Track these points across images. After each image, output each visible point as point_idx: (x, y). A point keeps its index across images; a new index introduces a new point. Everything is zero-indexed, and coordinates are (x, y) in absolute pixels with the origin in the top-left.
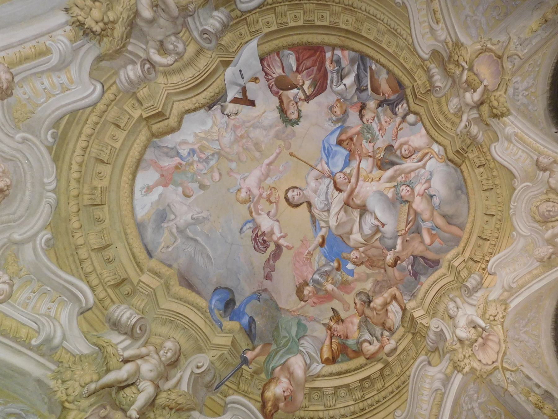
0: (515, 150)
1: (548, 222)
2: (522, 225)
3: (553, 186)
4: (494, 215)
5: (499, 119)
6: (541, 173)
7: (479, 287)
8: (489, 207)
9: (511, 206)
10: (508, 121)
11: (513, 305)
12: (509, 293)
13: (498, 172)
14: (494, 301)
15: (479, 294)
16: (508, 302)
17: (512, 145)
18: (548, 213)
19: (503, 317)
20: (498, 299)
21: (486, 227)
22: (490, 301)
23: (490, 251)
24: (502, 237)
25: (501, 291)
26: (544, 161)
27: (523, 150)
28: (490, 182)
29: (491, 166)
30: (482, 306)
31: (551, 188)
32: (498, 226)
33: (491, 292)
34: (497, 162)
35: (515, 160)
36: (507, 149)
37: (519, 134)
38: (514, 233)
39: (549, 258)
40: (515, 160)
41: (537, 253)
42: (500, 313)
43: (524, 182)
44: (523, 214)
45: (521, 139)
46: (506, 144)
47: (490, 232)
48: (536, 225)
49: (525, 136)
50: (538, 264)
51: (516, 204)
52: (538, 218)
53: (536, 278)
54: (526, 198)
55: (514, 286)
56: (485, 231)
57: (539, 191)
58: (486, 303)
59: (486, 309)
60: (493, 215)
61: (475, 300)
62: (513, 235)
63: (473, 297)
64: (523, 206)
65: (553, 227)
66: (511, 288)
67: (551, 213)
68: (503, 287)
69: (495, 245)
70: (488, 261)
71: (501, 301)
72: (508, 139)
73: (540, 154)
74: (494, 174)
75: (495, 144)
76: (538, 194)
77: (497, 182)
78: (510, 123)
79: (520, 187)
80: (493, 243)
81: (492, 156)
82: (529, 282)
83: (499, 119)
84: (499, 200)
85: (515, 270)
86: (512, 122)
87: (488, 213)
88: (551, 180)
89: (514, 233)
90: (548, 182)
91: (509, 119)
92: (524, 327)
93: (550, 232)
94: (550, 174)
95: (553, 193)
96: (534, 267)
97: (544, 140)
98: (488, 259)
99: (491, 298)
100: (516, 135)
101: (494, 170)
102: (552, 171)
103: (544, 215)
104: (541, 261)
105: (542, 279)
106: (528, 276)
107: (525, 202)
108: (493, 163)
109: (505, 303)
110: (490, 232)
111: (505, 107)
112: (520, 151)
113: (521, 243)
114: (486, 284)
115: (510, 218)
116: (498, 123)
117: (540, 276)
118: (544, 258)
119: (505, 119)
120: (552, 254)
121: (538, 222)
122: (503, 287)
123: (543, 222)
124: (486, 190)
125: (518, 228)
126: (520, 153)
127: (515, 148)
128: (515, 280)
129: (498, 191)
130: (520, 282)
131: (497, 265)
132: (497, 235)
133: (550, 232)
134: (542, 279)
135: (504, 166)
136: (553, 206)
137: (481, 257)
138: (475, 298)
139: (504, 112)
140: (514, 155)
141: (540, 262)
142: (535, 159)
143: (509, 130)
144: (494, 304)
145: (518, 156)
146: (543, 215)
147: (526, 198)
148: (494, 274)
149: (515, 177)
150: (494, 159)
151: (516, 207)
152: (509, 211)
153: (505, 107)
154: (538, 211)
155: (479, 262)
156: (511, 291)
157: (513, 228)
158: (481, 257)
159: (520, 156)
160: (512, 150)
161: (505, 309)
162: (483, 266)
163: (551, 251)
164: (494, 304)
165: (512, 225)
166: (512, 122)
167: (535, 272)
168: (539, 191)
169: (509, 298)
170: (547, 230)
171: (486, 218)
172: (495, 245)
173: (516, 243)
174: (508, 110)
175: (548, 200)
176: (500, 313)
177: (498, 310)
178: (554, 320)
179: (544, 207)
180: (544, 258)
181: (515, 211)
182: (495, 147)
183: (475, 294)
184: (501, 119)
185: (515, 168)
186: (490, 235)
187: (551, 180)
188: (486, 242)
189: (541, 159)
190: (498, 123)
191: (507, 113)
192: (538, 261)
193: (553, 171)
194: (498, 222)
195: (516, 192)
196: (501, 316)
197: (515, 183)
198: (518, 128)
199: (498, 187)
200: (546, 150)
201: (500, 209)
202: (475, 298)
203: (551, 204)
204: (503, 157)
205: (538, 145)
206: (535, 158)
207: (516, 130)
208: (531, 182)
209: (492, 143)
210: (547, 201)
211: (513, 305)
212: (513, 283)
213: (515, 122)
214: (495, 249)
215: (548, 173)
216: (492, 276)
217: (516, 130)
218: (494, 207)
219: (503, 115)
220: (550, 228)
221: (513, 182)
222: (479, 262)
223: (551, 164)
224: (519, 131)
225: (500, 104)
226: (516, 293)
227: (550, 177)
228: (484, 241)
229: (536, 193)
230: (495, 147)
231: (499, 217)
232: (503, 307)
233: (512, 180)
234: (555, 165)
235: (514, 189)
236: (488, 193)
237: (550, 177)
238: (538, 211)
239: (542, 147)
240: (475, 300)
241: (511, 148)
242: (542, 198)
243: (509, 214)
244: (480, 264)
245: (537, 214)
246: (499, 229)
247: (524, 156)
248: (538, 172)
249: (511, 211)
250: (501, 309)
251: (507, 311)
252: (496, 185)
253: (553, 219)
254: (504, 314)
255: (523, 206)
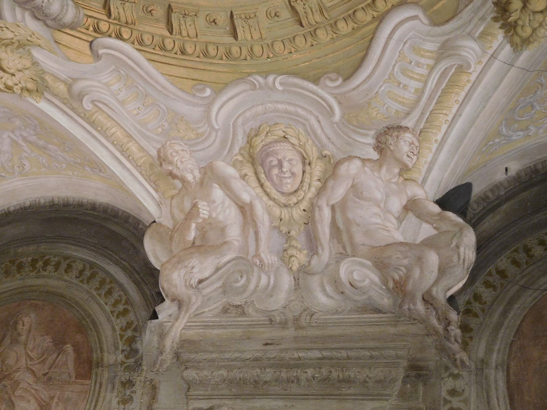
0: (419, 70)
1: (253, 163)
2: (233, 107)
3: (343, 169)
4: (235, 37)
5: (495, 19)
6: (371, 141)
7: (49, 22)
8: (251, 21)
9: (271, 78)
10: (495, 45)
11: (43, 105)
12: (68, 97)
13: (345, 36)
14: (35, 63)
15: (33, 25)
16: (46, 94)
17: (431, 62)
18: (275, 162)
19: (9, 88)
20: (44, 72)
21: (201, 22)
22: (30, 54)
23: (147, 39)
24: (189, 64)
25: (63, 76)
26: (404, 144)
27: (423, 92)
28: (318, 17)
29: (360, 15)
30: (10, 35)
31: (338, 164)
32: (212, 51)
33: (50, 51)
34: (376, 29)
35: (392, 74)
36: (416, 49)
37: (464, 78)
38: (208, 92)
39: (173, 176)
40: (392, 74)
41: (177, 148)
42: (15, 80)
43: (340, 103)
44: (260, 109)
45: (452, 84)
46: (431, 46)
47: (192, 33)
48: (241, 140)
49: (463, 94)
50: (154, 153)
51: (280, 88)
52: (259, 142)
53: (122, 152)
54: (300, 111)
55: (87, 105)
56: (188, 19)
57: (325, 140)
58: (21, 45)
59: (7, 45)
60: (235, 35)
61: (14, 16)
62: (203, 90)
63: (18, 10)
64: (280, 106)
65: (244, 177)
66: (80, 97)
67: (275, 171)
68: (75, 80)
69: (163, 48)
70: (119, 37)
71: (43, 79)
72: (445, 50)
73: (422, 134)
74: (341, 25)
75: (421, 16)
76: (315, 134)
77: (321, 33)
78: (491, 52)
79: (326, 91)
80: (169, 43)
81: (388, 12)
82: (107, 138)
83: (495, 19)
84: (278, 46)
85: (122, 103)
86: (493, 56)
87: (238, 23)
88: (357, 163)
89: (208, 92)
90: (350, 158)
91: (501, 47)
92: (25, 139)
93: (231, 171)
94: (369, 160)
95: (325, 172)
96: (144, 143)
97: (461, 138)
98: (126, 36)
99: (37, 54)
100: (461, 69)
101: (351, 24)
102: (379, 164)
103: (268, 155)
104: (162, 159)
105: (120, 162)
106: (119, 134)
107: (291, 108)
108: (369, 18)
109: (40, 87)
110: (192, 33)
111: (534, 30)
112: (419, 85)
113: (194, 112)
114: (59, 36)
115: (243, 77)
116: (483, 19)
117: (128, 158)
118: (170, 163)
119: (500, 35)
120: (183, 180)
121: (250, 142)
122: (75, 80)
123: (251, 156)
124: (293, 8)
125: (224, 98)
126: (414, 85)
127: (424, 71)
128: (96, 103)
129: (300, 41)
130: (100, 117)
131: (119, 59)
132: (189, 50)
133: (231, 171)
134: (120, 162)
135: (368, 48)
136: (293, 174)
137: (123, 20)
138: (19, 16)
139: (519, 29)
140: (404, 72)
141: (159, 157)
142: (404, 123)
143: (470, 49)
144: (28, 64)
145: (404, 80)
146: (266, 152)
147: (300, 111)
148: (97, 57)
149: (347, 78)
150: (381, 19)
151: (273, 88)
152: (259, 73)
153: (534, 30)
154: (276, 142)
155: (109, 15)
156: (73, 99)
157: (220, 88)
158: (123, 20)
159: (405, 87)
160: (418, 64)
161: (28, 90)
162: (104, 27)
163: (189, 177)
164: (28, 64)
165: (226, 85)
166: (493, 56)
167: (134, 148)
168: (325, 140)
169: (56, 95)
170: (234, 166)
171: (223, 19)
172: (163, 48)
173: (190, 98)
174: (526, 42)
175: (305, 161)
176: (15, 80)
177: (19, 75)
178: (71, 200)
179: (286, 153)
180: (170, 163)
181: (261, 88)
182: (415, 17)
183: (27, 15)
184: (498, 25)
185: (369, 77)
186: (184, 33)
187: (357, 163)
188: (163, 25)
189: (408, 136)
190: (483, 19)
191: (517, 40)
192: (159, 151)
193: (381, 166)
194: (222, 49)
195: (311, 86)
196: (10, 83)
197: (332, 80)
198: (483, 73)
199: (309, 39)
200: (434, 147)
201: (257, 50)
202: (19, 16)
203: (298, 168)
204: (392, 43)
205: (444, 127)
206: (409, 123)
207: (475, 69)
208: (342, 117)
209: (425, 9)
210: (304, 159)
211: (43, 105)
212: (93, 102)
213: (496, 64)
214: (156, 50)
215: (374, 155)
216: (88, 52)
217: (475, 69)
218: (256, 36)
219: (510, 28)
220: (239, 170)
221: (333, 76)
222: (109, 15)
223: (399, 161)
224: (473, 78)
225: (539, 17)
226: (73, 109)
227: (363, 160)
228: (165, 21)
229: (319, 132)
230: (415, 17)
231: (235, 50)
232: (30, 85)
233: (338, 71)
234: (397, 170)
235: (316, 81)
236: (286, 14)
237: (363, 160)
238: (276, 142)
239: (439, 137)
240: (14, 16)
241: (422, 60)
242: (308, 147)
243: (250, 74)
244: (105, 18)
245: (269, 140)
246: (206, 54)
247: (409, 96)
248: (372, 133)
249: (261, 79)
250: (23, 79)
251: (26, 94)
252: (313, 34)
253: (262, 176)
254: (17, 89)
255: (280, 106)
